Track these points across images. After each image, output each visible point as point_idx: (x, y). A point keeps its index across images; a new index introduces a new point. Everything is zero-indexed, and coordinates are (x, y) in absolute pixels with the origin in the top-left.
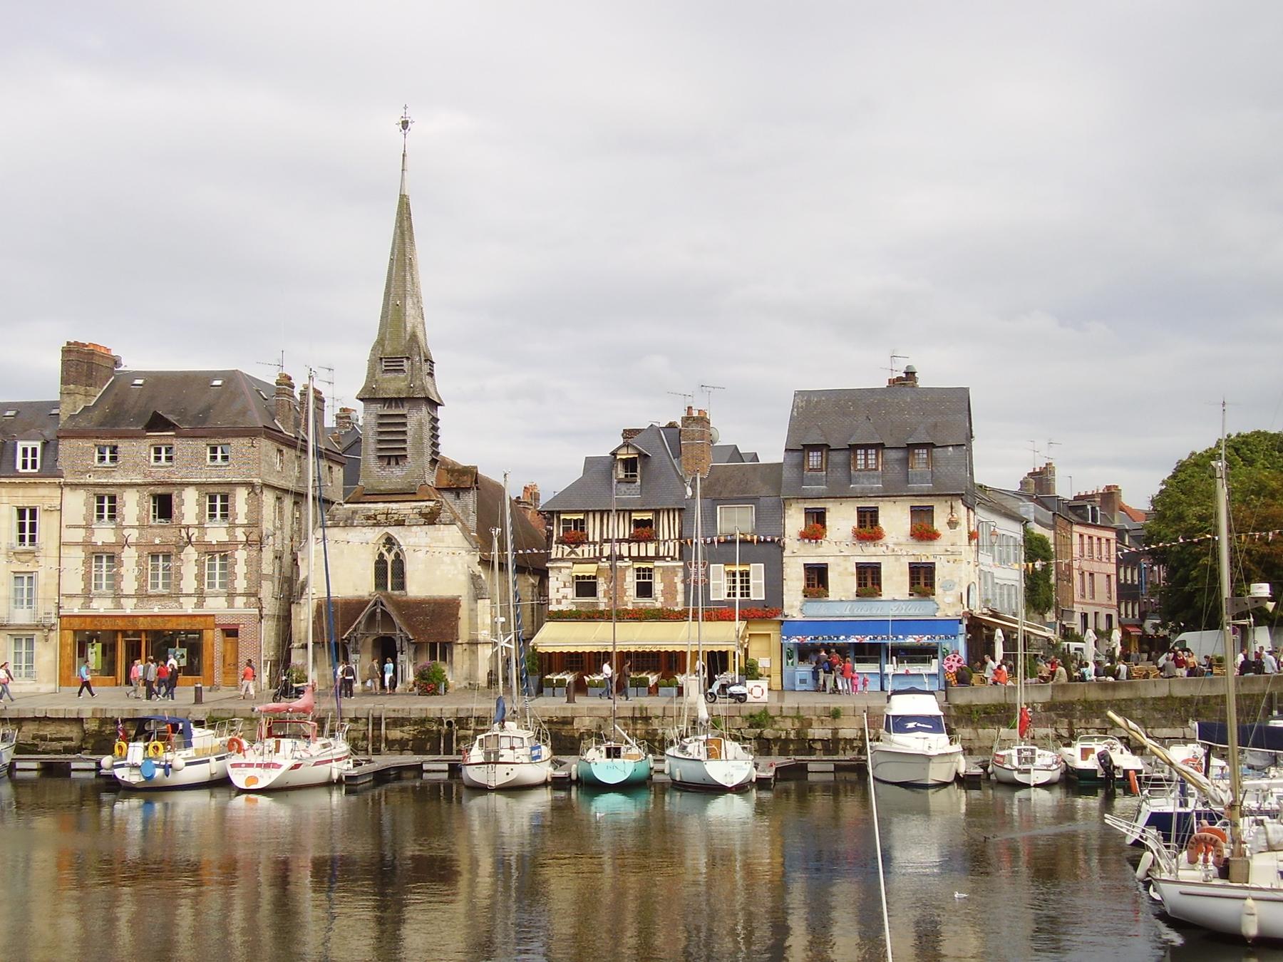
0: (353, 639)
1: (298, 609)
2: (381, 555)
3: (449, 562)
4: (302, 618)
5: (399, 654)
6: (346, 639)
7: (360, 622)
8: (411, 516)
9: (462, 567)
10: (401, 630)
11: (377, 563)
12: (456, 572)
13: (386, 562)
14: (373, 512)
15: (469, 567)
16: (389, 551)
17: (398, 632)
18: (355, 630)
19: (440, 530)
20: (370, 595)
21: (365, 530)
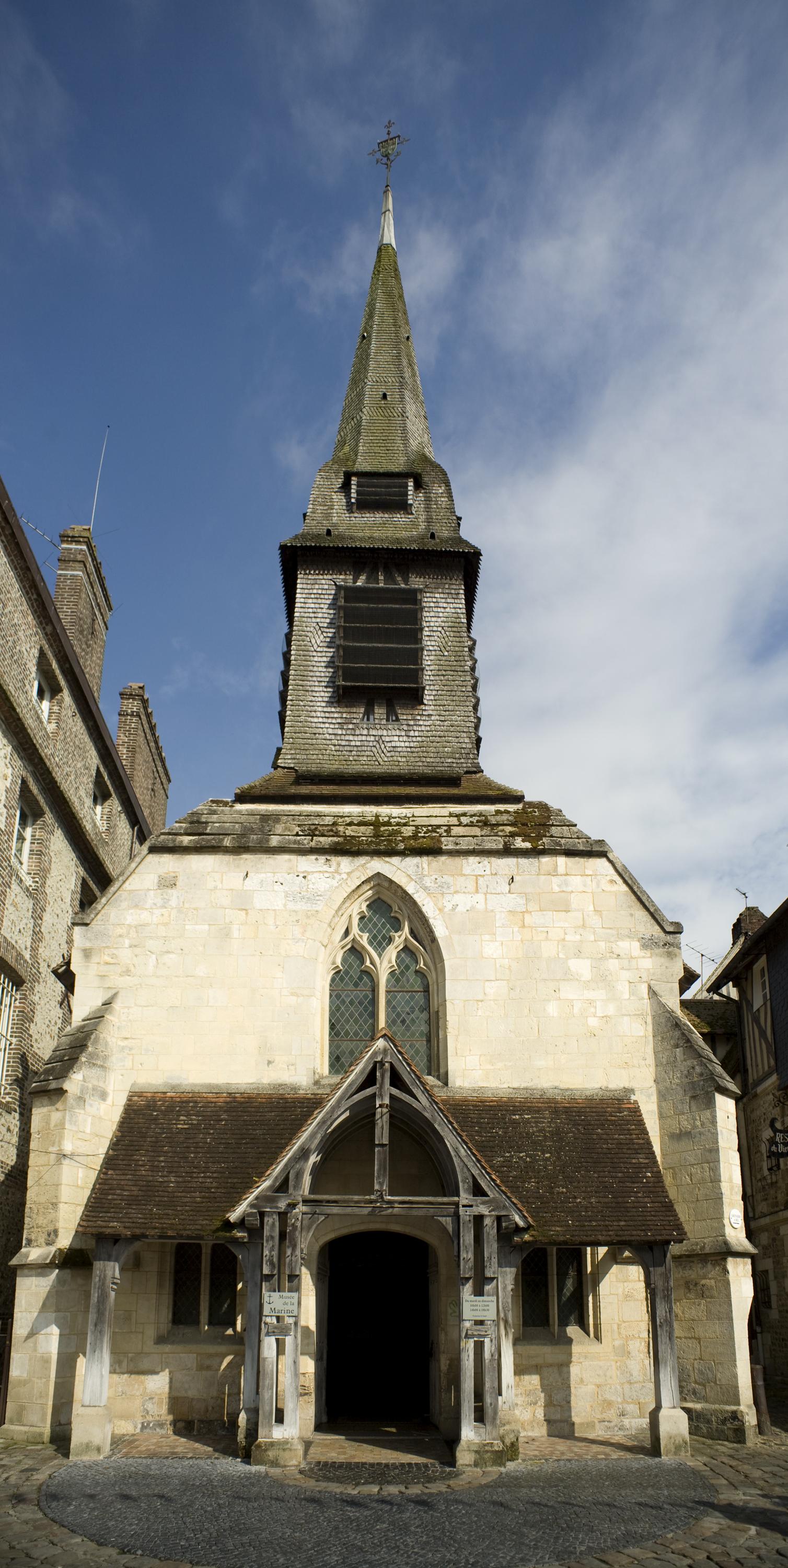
0: (271, 1226)
1: (55, 1116)
2: (355, 952)
3: (587, 974)
4: (68, 1147)
5: (467, 1291)
6: (242, 1223)
7: (304, 1154)
8: (456, 831)
9: (632, 993)
10: (478, 1191)
11: (338, 978)
12: (611, 1010)
13: (369, 976)
14: (328, 820)
15: (653, 993)
16: (381, 942)
17: (465, 1197)
18: (283, 1186)
19: (554, 873)
20: (316, 1083)
21: (306, 863)
